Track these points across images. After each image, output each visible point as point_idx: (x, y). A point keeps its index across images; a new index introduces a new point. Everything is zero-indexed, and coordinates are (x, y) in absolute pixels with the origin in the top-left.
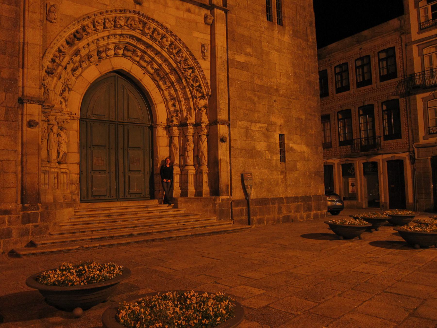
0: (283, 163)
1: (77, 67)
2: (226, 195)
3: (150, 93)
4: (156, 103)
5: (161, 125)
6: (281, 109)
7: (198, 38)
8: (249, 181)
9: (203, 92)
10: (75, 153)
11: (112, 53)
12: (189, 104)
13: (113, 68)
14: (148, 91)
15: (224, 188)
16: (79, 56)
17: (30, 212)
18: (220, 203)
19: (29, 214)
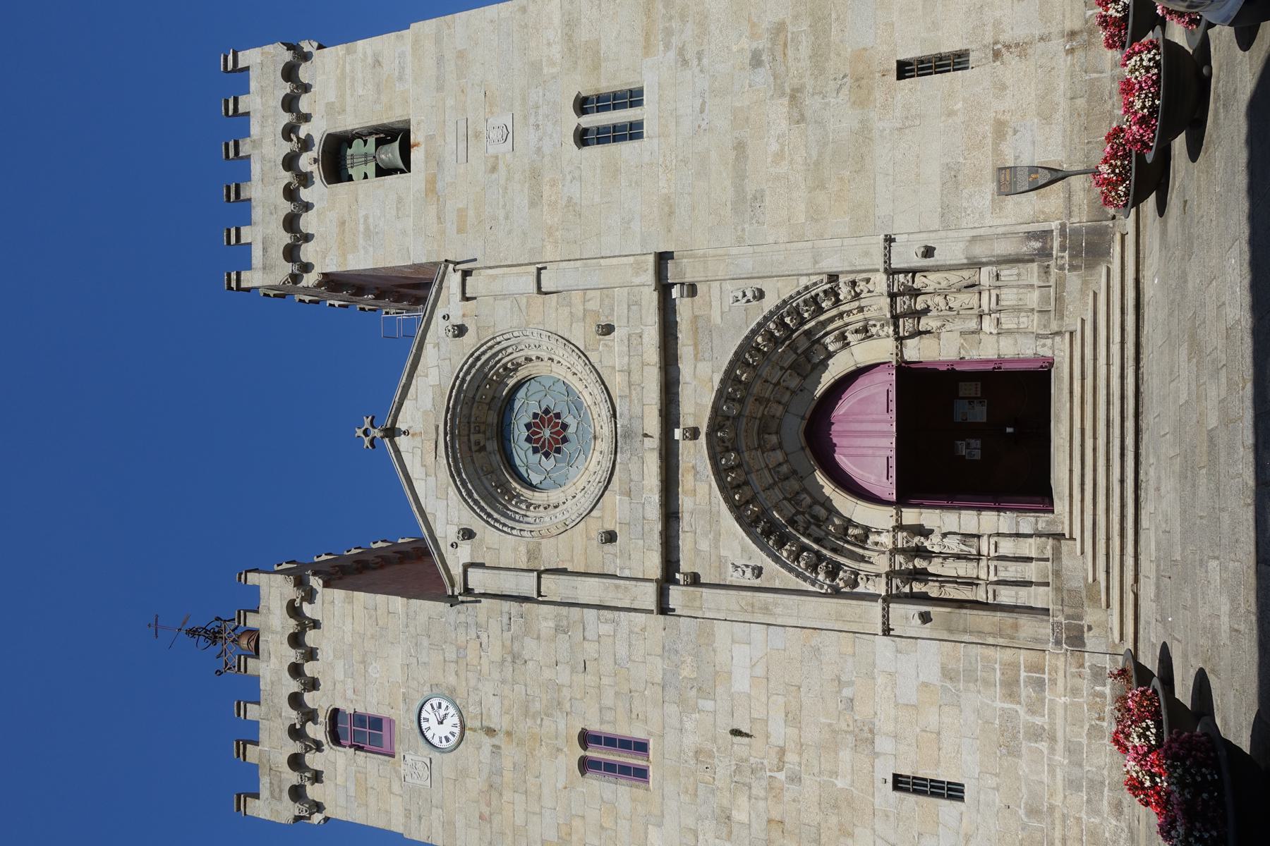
0: (973, 57)
1: (813, 517)
2: (1052, 239)
3: (836, 378)
4: (853, 363)
5: (897, 355)
6: (835, 79)
7: (722, 313)
8: (1018, 176)
9: (825, 292)
10: (960, 518)
11: (779, 456)
12: (849, 312)
13: (803, 449)
14: (833, 380)
15: (1037, 245)
16: (795, 518)
17: (1064, 635)
18: (1071, 256)
19: (1067, 638)
